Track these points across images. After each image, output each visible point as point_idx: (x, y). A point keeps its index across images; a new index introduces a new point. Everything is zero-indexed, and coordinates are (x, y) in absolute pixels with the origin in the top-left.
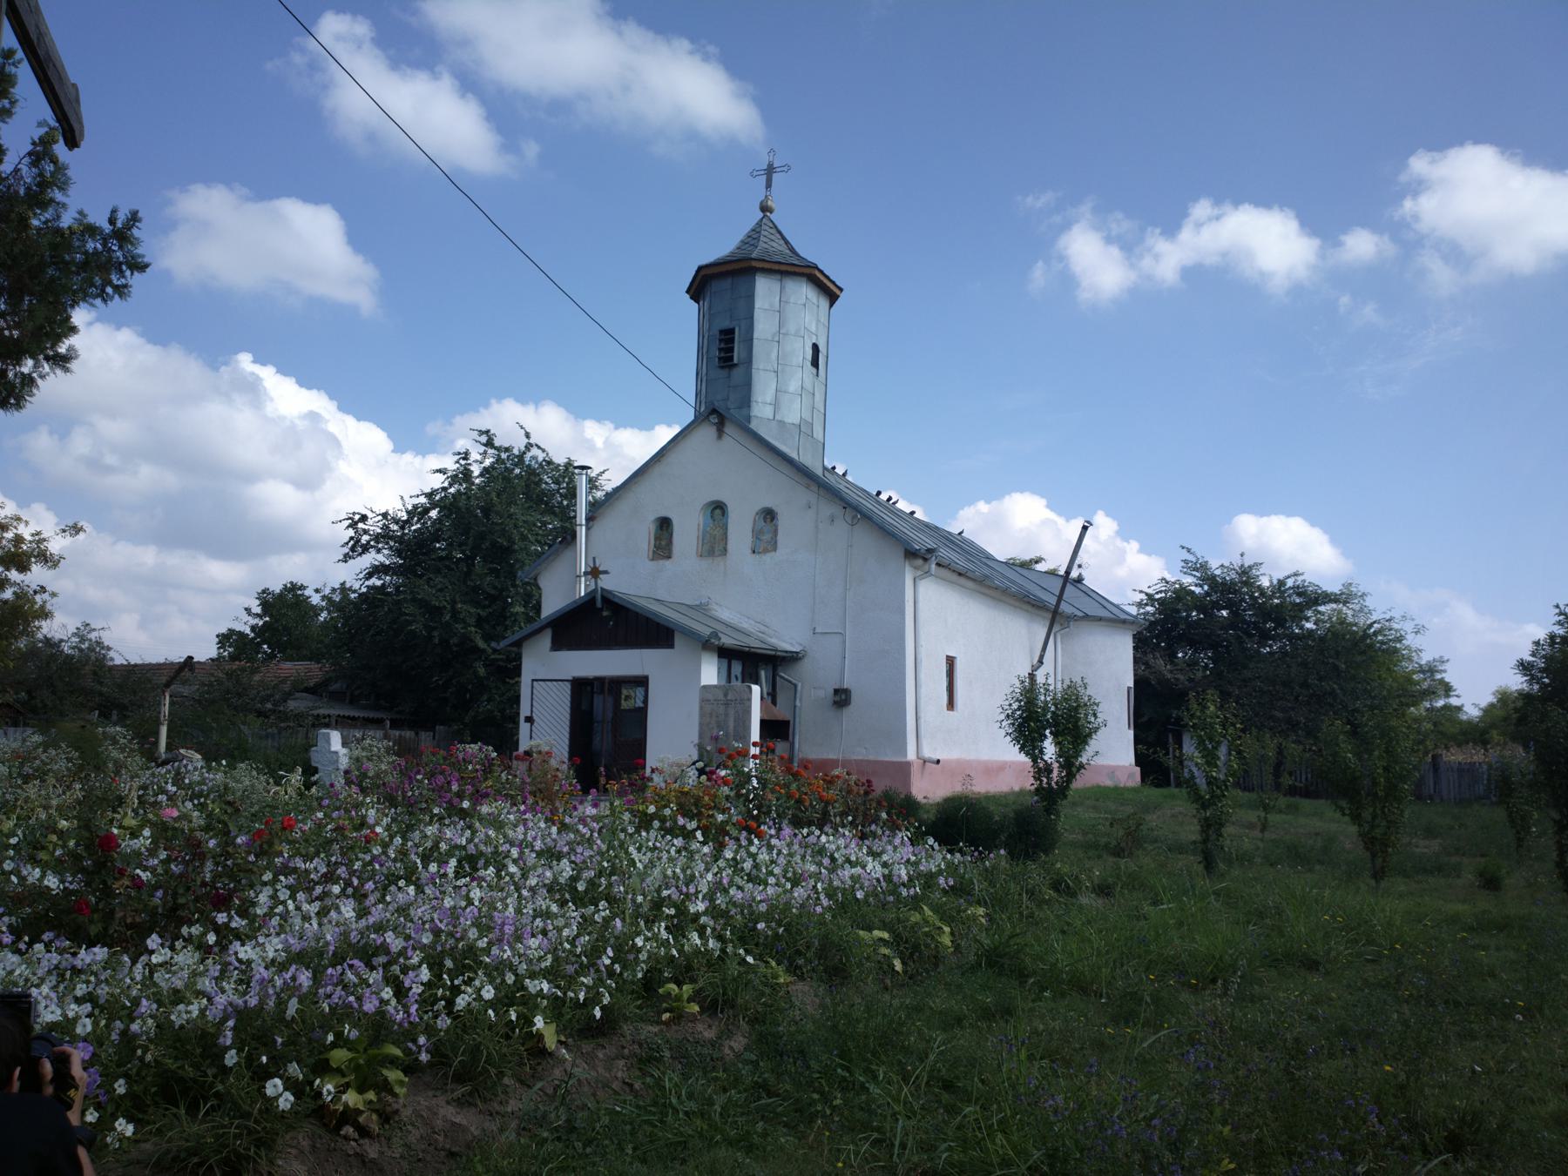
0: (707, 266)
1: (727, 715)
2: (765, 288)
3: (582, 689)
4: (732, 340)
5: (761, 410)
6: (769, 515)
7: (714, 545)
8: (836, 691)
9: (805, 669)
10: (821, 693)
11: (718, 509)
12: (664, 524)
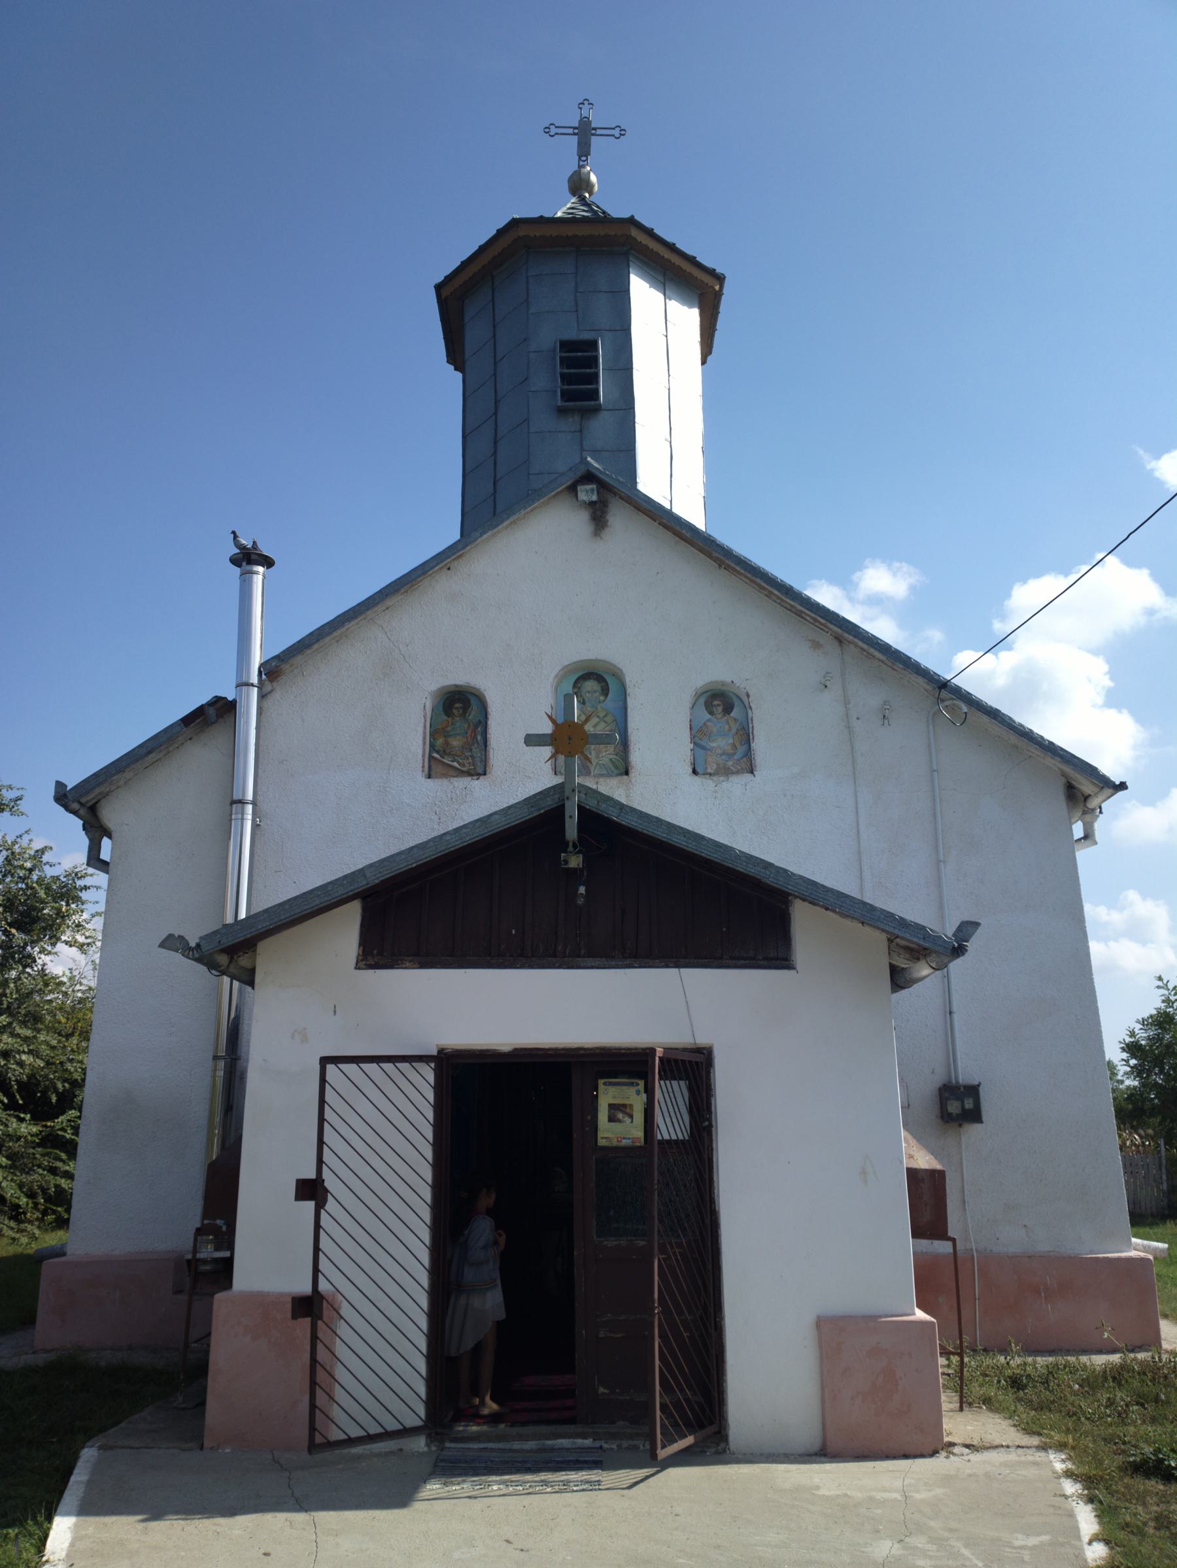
0: (449, 279)
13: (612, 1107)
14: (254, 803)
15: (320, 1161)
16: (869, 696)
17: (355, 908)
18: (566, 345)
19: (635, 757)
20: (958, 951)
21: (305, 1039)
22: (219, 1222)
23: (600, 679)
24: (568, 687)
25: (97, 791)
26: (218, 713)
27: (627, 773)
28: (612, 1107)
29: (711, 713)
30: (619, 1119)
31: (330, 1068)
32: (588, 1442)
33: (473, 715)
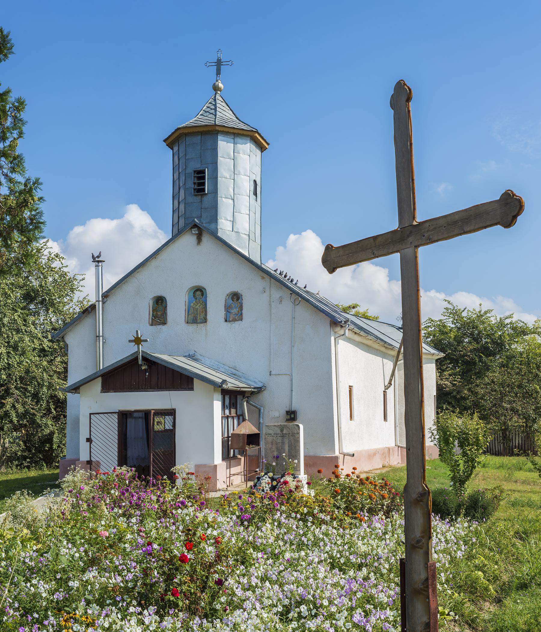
1: (283, 443)
2: (224, 146)
3: (124, 417)
4: (204, 178)
5: (224, 226)
6: (236, 297)
7: (197, 315)
8: (288, 413)
9: (265, 396)
10: (277, 414)
11: (199, 292)
12: (160, 302)
14: (103, 336)
15: (90, 435)
16: (276, 294)
17: (100, 379)
19: (209, 317)
23: (201, 291)
24: (192, 294)
27: (206, 322)
29: (233, 301)
30: (161, 424)
31: (92, 415)
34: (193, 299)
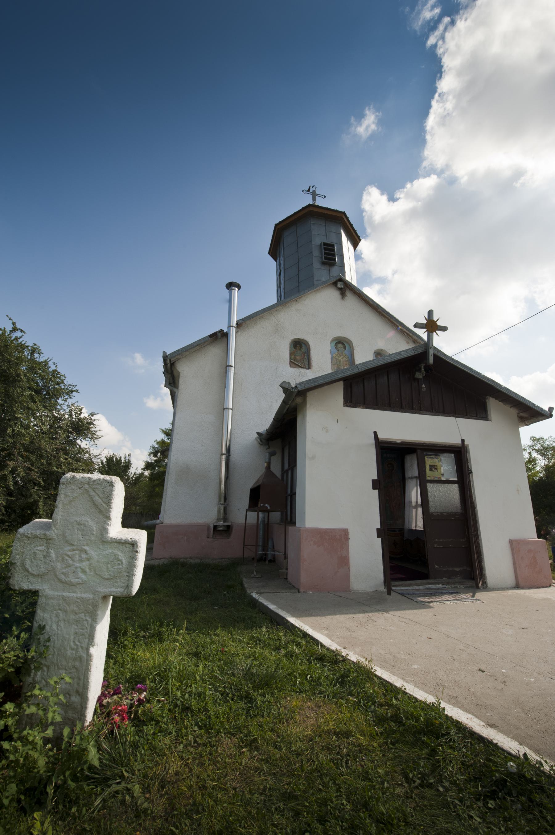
13: (430, 465)
18: (325, 244)
20: (551, 416)
21: (327, 431)
22: (267, 505)
25: (177, 357)
26: (220, 337)
28: (430, 465)
32: (440, 585)
33: (304, 349)
34: (335, 350)
